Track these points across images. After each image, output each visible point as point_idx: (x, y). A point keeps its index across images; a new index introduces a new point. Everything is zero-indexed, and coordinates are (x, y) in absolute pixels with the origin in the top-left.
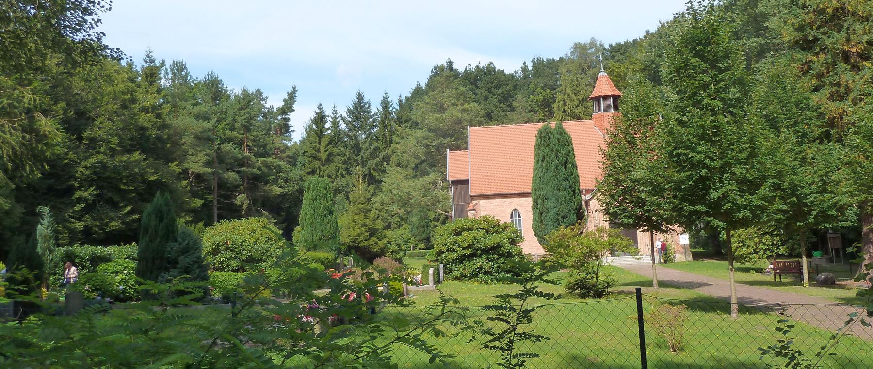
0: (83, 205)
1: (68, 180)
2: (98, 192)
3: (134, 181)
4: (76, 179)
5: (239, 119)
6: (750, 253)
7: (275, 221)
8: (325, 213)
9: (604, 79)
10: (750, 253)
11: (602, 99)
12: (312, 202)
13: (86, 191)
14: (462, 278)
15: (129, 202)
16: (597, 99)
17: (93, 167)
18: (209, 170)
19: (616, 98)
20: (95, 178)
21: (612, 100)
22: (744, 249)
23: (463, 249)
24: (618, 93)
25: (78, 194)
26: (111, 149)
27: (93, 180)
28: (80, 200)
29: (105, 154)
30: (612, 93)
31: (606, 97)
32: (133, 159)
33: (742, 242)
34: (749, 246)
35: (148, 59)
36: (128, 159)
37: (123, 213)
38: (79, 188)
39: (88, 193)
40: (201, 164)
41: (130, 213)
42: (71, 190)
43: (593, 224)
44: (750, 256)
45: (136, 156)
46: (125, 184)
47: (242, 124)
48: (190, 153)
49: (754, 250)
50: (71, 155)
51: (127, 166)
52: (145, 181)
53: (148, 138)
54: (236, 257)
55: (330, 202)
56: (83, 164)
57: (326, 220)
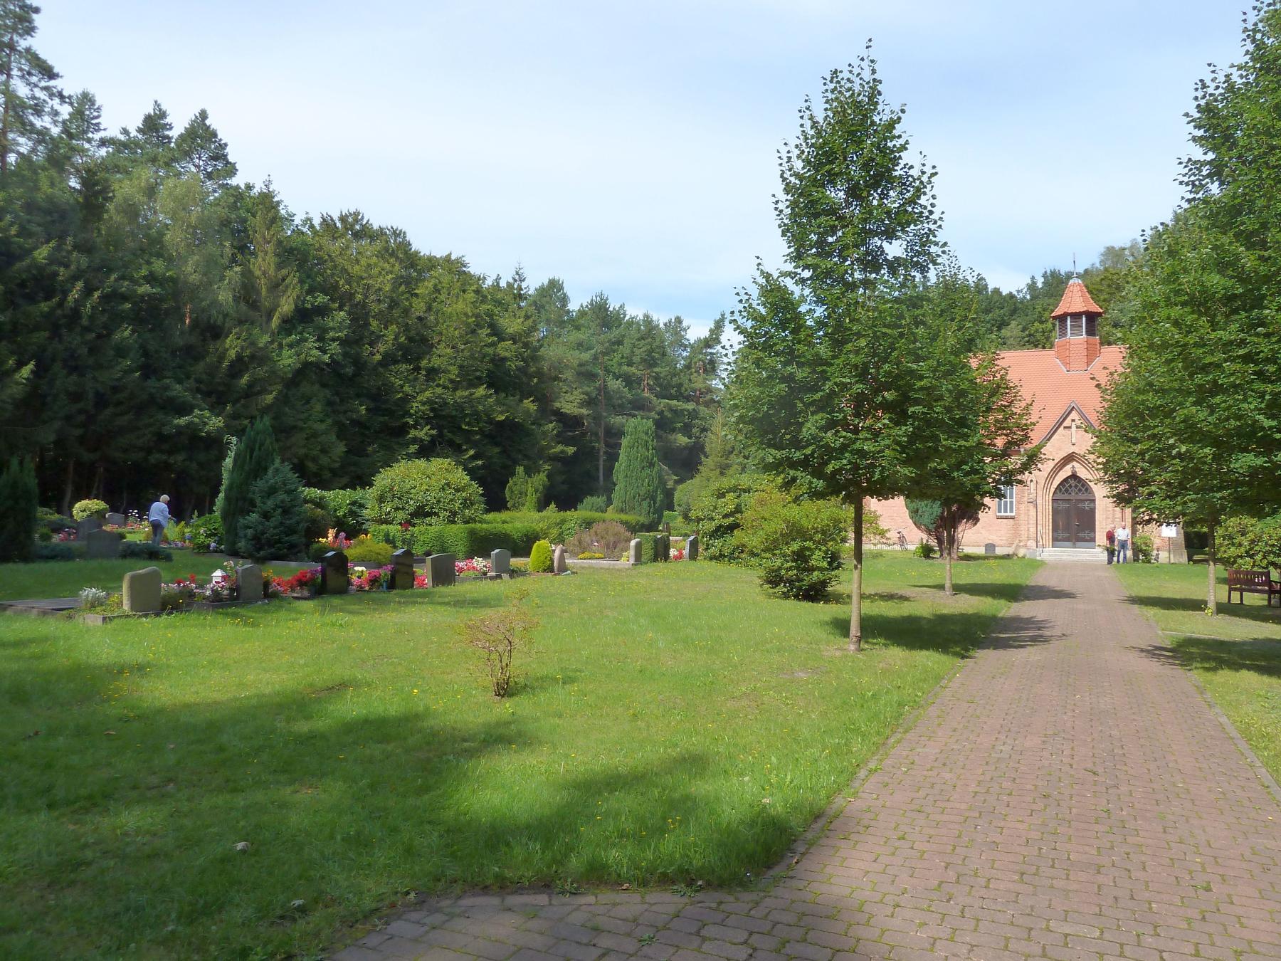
0: (417, 447)
1: (403, 416)
2: (434, 432)
3: (478, 420)
4: (411, 416)
5: (637, 351)
6: (1241, 557)
7: (676, 478)
8: (643, 464)
9: (1076, 289)
10: (1238, 556)
11: (1069, 318)
12: (629, 449)
13: (421, 430)
14: (719, 557)
15: (474, 445)
16: (1062, 318)
17: (429, 401)
18: (584, 411)
19: (1092, 317)
20: (432, 414)
21: (1084, 319)
22: (1233, 549)
23: (723, 518)
24: (1095, 308)
25: (413, 433)
26: (452, 381)
27: (429, 418)
28: (415, 440)
29: (445, 387)
30: (1085, 309)
31: (1076, 316)
32: (478, 394)
33: (1231, 538)
34: (1240, 545)
35: (517, 277)
36: (471, 394)
37: (465, 457)
38: (415, 427)
39: (424, 433)
40: (575, 404)
41: (473, 458)
42: (404, 429)
43: (1026, 499)
44: (1240, 561)
45: (481, 391)
46: (468, 424)
47: (641, 358)
48: (564, 390)
49: (1247, 552)
50: (407, 388)
51: (470, 400)
52: (491, 421)
53: (507, 373)
54: (403, 508)
55: (650, 452)
56: (419, 398)
57: (644, 474)
